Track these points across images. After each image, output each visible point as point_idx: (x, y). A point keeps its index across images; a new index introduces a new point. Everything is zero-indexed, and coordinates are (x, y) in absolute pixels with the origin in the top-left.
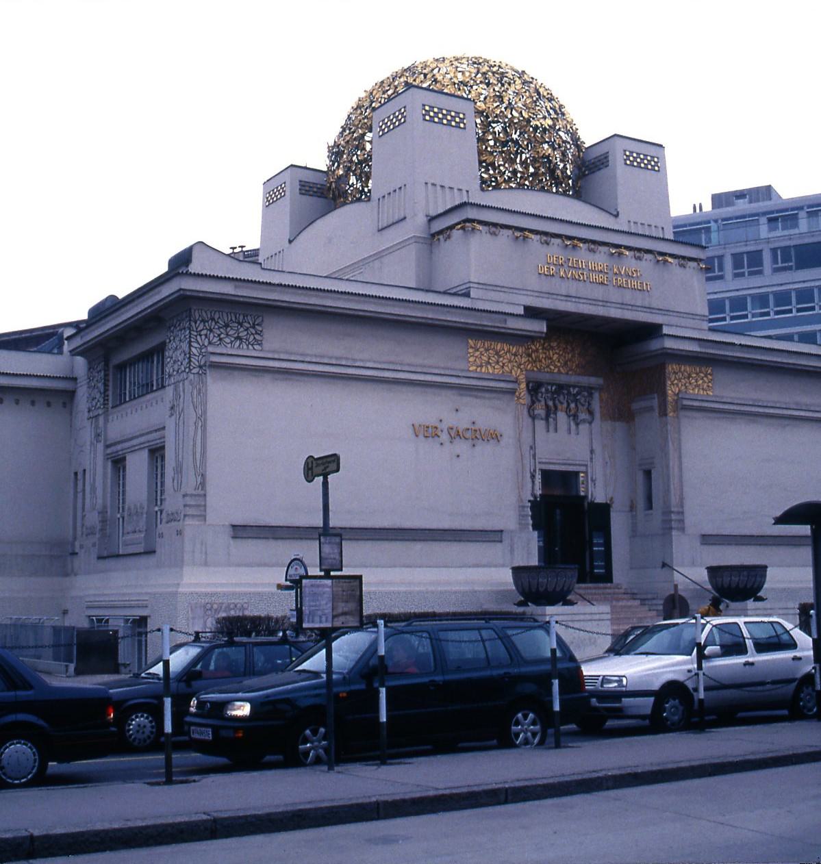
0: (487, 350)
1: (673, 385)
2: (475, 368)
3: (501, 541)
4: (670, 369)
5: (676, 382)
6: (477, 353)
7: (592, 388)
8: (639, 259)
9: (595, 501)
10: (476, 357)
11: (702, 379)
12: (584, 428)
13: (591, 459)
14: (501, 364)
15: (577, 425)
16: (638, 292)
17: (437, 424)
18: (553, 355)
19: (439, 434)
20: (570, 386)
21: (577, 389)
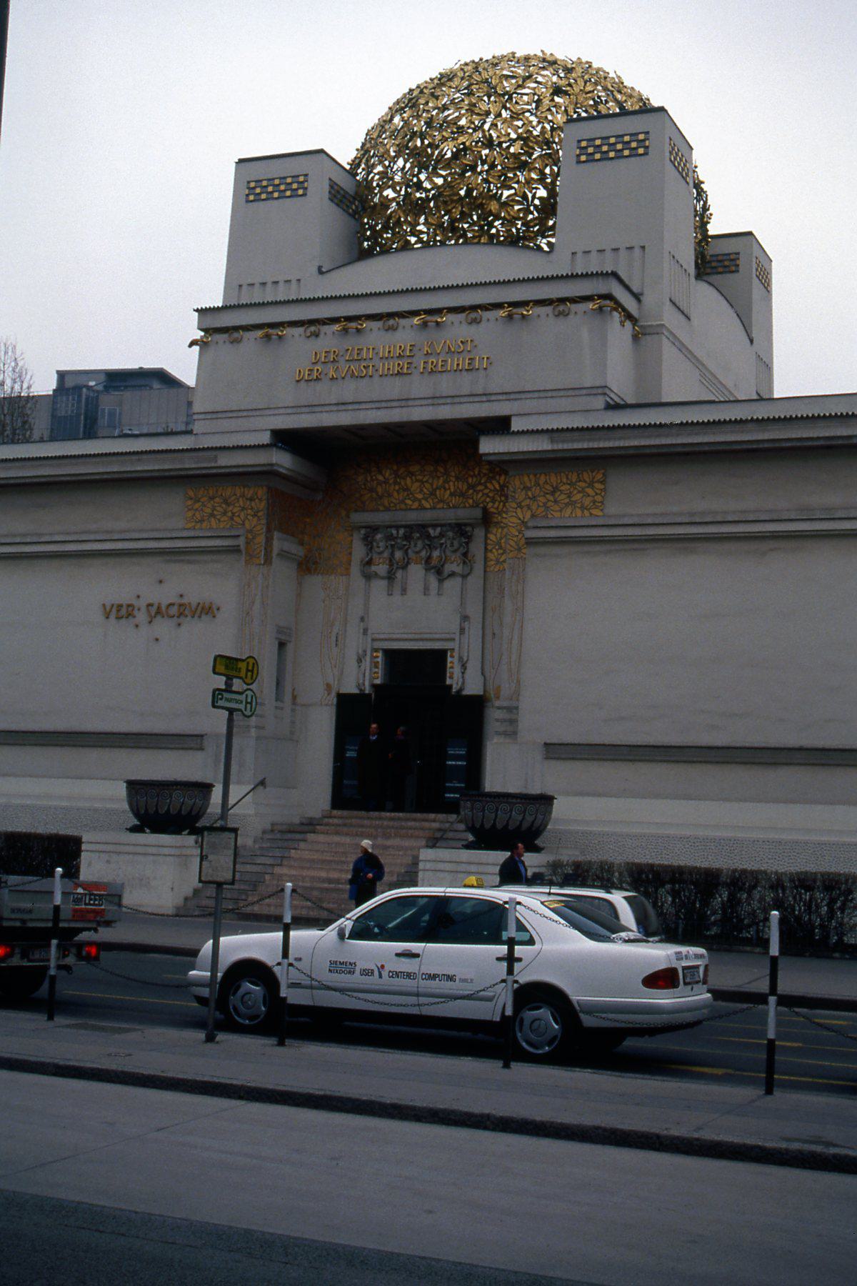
0: (212, 498)
1: (521, 508)
2: (193, 524)
3: (202, 749)
4: (517, 483)
5: (527, 502)
6: (197, 506)
7: (466, 525)
8: (476, 321)
9: (465, 692)
10: (197, 509)
11: (582, 491)
12: (452, 585)
13: (462, 631)
14: (230, 514)
15: (441, 581)
16: (465, 373)
17: (134, 602)
18: (412, 483)
19: (136, 612)
20: (424, 526)
21: (439, 529)
